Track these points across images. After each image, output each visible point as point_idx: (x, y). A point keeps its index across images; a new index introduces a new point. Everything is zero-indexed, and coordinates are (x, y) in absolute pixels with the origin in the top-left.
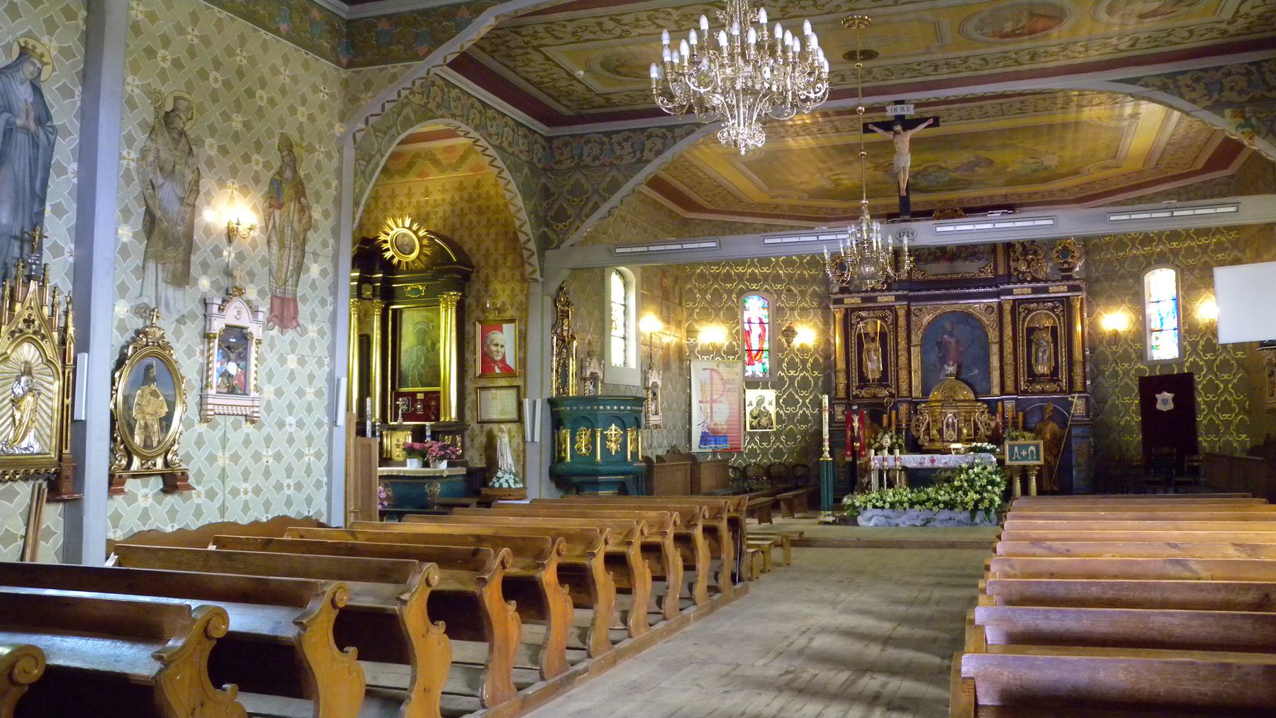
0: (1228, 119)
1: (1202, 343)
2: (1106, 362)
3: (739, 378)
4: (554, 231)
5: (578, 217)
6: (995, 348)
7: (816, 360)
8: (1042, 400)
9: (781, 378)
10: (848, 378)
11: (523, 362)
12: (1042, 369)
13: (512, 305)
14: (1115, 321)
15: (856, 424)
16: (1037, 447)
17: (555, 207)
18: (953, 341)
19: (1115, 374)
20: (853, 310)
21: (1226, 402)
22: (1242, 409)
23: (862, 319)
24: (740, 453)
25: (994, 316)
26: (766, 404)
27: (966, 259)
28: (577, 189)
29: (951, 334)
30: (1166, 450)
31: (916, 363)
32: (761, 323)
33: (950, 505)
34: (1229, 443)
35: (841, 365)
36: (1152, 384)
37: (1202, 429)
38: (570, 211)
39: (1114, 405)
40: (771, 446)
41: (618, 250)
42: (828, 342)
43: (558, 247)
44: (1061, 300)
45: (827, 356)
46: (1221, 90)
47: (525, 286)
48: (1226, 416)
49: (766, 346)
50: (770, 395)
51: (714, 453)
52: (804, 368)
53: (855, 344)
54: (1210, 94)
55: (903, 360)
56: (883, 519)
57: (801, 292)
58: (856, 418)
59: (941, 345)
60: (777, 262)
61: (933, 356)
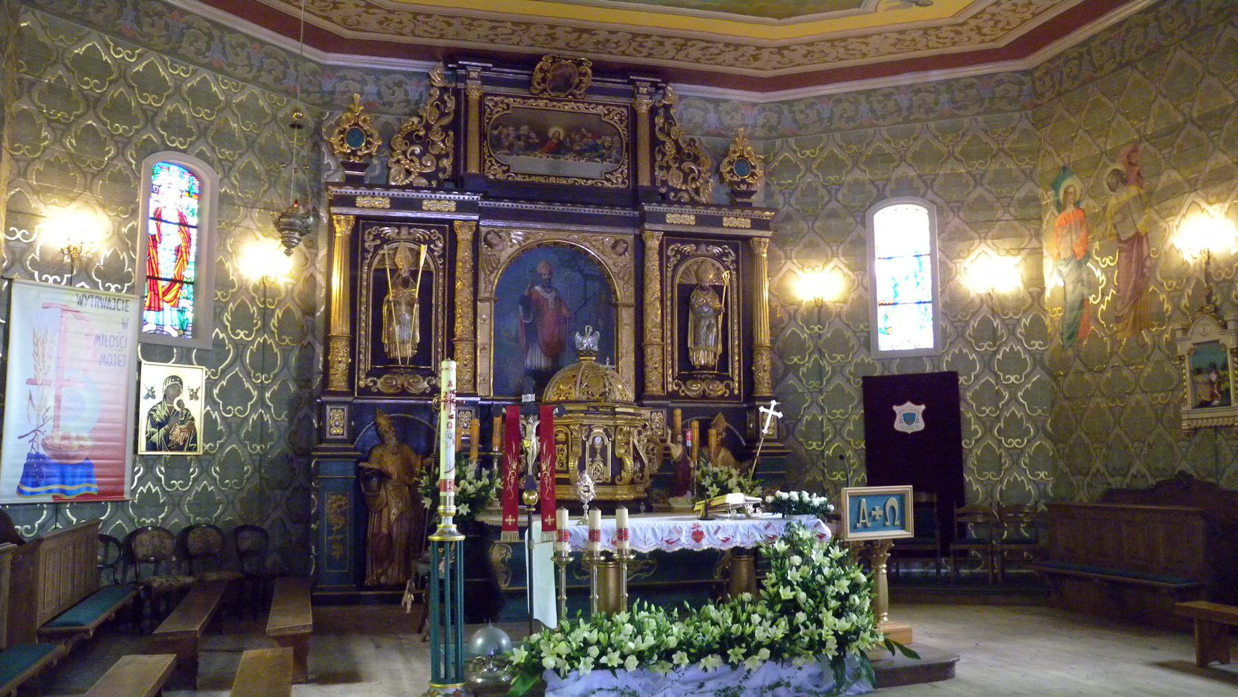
1: (1026, 321)
2: (801, 349)
3: (130, 334)
6: (626, 317)
7: (287, 312)
9: (219, 344)
10: (352, 354)
12: (701, 357)
14: (812, 282)
15: (532, 443)
16: (902, 497)
18: (549, 297)
19: (819, 372)
22: (1040, 429)
23: (386, 241)
24: (120, 504)
25: (628, 259)
26: (184, 396)
27: (580, 154)
29: (548, 286)
32: (183, 223)
34: (1015, 484)
35: (340, 326)
36: (885, 388)
37: (971, 462)
40: (195, 484)
42: (311, 279)
45: (309, 311)
49: (189, 274)
50: (194, 377)
51: (57, 507)
52: (265, 328)
53: (370, 291)
55: (461, 327)
57: (268, 172)
58: (532, 426)
59: (529, 303)
60: (228, 104)
61: (515, 324)
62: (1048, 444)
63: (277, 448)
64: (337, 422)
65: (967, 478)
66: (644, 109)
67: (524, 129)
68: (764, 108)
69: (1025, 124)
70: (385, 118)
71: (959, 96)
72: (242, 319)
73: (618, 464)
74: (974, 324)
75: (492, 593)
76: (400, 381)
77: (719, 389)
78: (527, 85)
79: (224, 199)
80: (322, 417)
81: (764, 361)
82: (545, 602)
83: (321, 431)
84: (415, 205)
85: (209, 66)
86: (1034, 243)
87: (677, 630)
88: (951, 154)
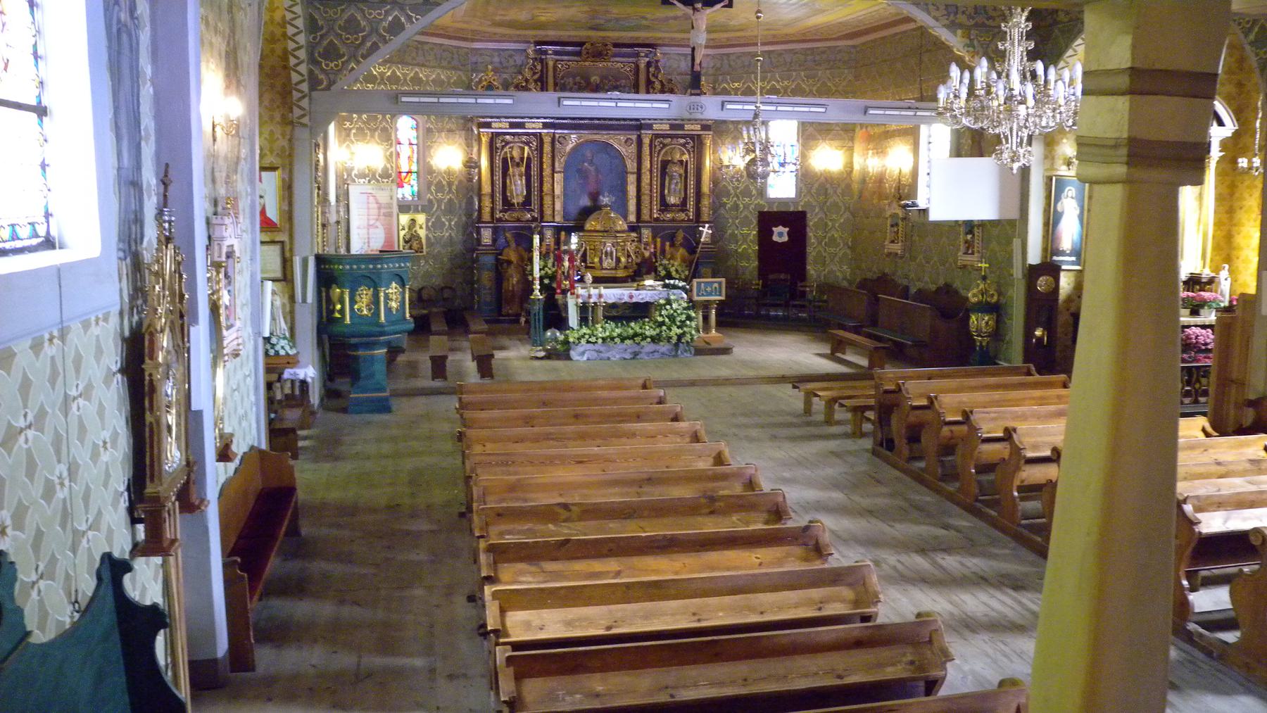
0: (959, 39)
2: (728, 195)
4: (323, 70)
5: (353, 57)
8: (675, 228)
9: (430, 201)
10: (493, 202)
11: (289, 215)
12: (672, 200)
13: (271, 151)
14: (733, 157)
15: (566, 264)
16: (720, 283)
17: (325, 43)
18: (592, 169)
19: (736, 207)
20: (498, 134)
21: (833, 239)
23: (507, 143)
28: (351, 25)
29: (591, 163)
30: (782, 276)
31: (558, 190)
33: (655, 339)
35: (486, 188)
36: (769, 218)
38: (343, 50)
39: (733, 235)
41: (404, 99)
43: (328, 88)
44: (692, 137)
46: (956, 13)
47: (289, 128)
48: (832, 250)
49: (414, 168)
50: (421, 218)
53: (503, 167)
54: (948, 15)
55: (546, 187)
56: (595, 354)
58: (566, 258)
59: (583, 174)
62: (849, 252)
63: (459, 248)
64: (487, 236)
65: (808, 267)
66: (642, 66)
67: (578, 79)
68: (713, 57)
69: (850, 77)
70: (505, 76)
71: (817, 58)
72: (440, 187)
73: (618, 260)
74: (816, 185)
75: (556, 318)
76: (515, 215)
77: (682, 216)
78: (578, 54)
79: (429, 131)
80: (479, 233)
81: (706, 202)
82: (573, 318)
83: (479, 241)
84: (521, 125)
85: (418, 65)
86: (850, 144)
87: (618, 331)
88: (811, 91)
